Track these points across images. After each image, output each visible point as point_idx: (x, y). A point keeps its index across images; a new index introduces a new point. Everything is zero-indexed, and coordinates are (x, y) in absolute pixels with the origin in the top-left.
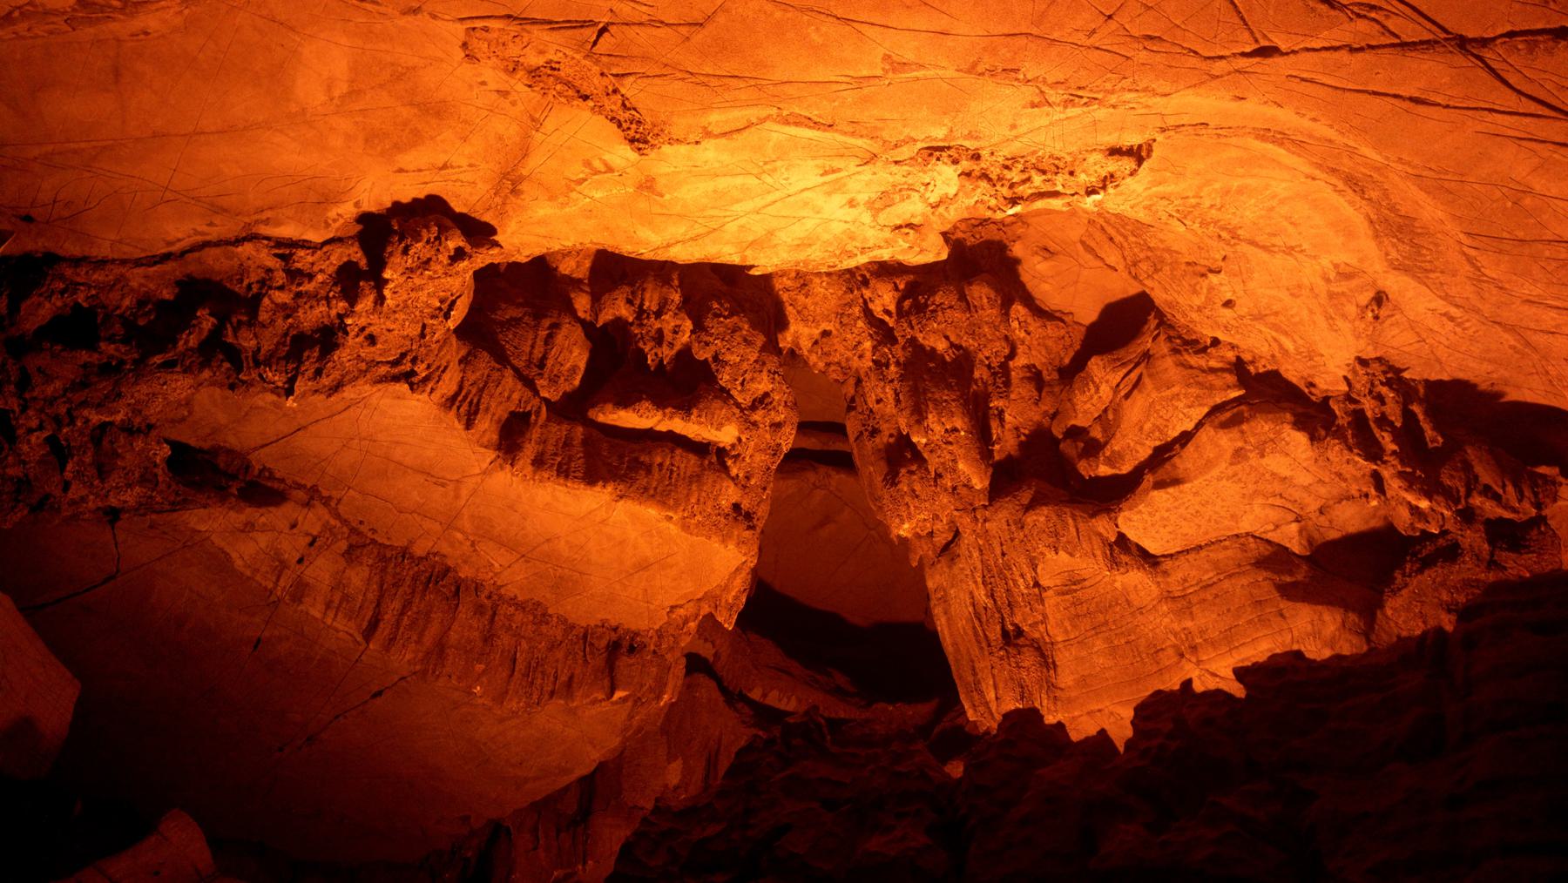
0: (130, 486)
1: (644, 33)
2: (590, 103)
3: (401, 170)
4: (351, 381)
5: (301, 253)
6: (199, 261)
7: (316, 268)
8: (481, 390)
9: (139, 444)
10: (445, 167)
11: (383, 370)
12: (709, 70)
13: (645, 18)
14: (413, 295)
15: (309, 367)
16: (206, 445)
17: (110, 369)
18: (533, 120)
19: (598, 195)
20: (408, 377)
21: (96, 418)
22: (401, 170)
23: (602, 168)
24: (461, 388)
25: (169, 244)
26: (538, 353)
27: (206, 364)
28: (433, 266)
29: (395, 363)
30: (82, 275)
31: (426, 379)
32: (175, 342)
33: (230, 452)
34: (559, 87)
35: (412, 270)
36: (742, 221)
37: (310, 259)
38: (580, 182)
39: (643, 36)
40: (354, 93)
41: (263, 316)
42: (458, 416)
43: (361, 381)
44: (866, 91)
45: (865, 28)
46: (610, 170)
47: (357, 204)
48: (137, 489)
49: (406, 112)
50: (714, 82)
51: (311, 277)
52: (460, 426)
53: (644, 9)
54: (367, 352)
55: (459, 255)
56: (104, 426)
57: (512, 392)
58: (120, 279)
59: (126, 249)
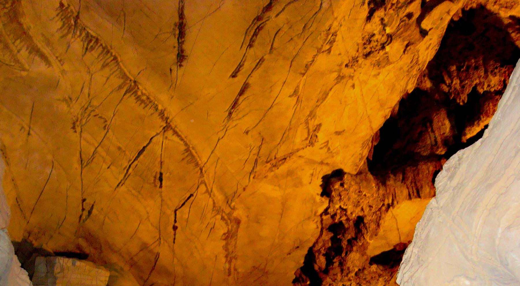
0: (378, 280)
1: (262, 150)
2: (288, 158)
3: (310, 183)
4: (380, 220)
5: (329, 210)
6: (326, 225)
7: (335, 210)
8: (415, 183)
9: (366, 272)
10: (312, 175)
11: (384, 208)
12: (279, 140)
13: (258, 149)
14: (351, 200)
15: (364, 231)
16: (392, 248)
17: (341, 264)
18: (300, 156)
19: (338, 144)
20: (389, 206)
21: (353, 274)
22: (310, 183)
23: (326, 144)
24: (408, 188)
25: (318, 228)
26: (433, 139)
27: (352, 247)
28: (342, 194)
29: (383, 205)
30: (317, 248)
31: (393, 200)
32: (342, 247)
33: (397, 245)
34: (281, 162)
35: (341, 199)
36: (368, 109)
37: (332, 210)
38: (329, 149)
39: (263, 151)
40: (279, 186)
41: (346, 226)
42: (416, 197)
43: (383, 216)
44: (303, 99)
45: (276, 102)
46: (328, 142)
47: (318, 194)
48: (381, 279)
49: (289, 178)
50: (284, 139)
51: (335, 214)
52: (419, 199)
53: (255, 148)
54: (373, 210)
55: (342, 185)
56: (356, 274)
57: (428, 169)
58: (324, 241)
59: (315, 235)
